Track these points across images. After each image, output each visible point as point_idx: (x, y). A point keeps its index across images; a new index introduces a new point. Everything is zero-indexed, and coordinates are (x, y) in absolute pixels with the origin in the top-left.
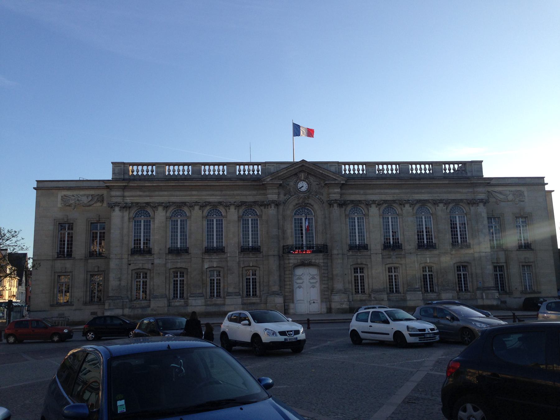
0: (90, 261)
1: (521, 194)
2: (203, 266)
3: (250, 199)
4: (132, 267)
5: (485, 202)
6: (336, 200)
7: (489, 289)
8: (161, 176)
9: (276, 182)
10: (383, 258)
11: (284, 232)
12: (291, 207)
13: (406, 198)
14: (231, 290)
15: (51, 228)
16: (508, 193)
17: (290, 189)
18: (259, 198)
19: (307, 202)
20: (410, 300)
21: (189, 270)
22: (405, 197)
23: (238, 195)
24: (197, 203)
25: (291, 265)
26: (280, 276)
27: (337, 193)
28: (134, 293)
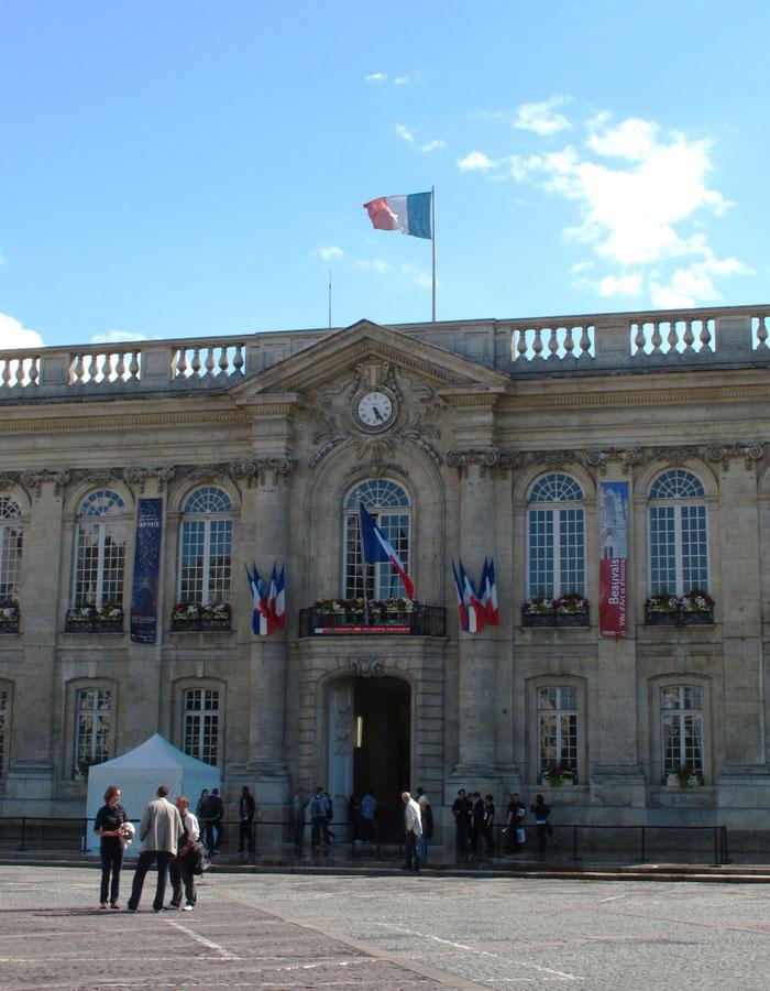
2: (56, 674)
3: (207, 457)
6: (472, 452)
9: (274, 399)
10: (640, 655)
12: (336, 479)
13: (731, 438)
17: (333, 419)
18: (231, 453)
19: (387, 459)
20: (729, 808)
21: (19, 688)
22: (726, 433)
23: (169, 445)
24: (47, 473)
25: (315, 675)
26: (285, 713)
27: (483, 426)
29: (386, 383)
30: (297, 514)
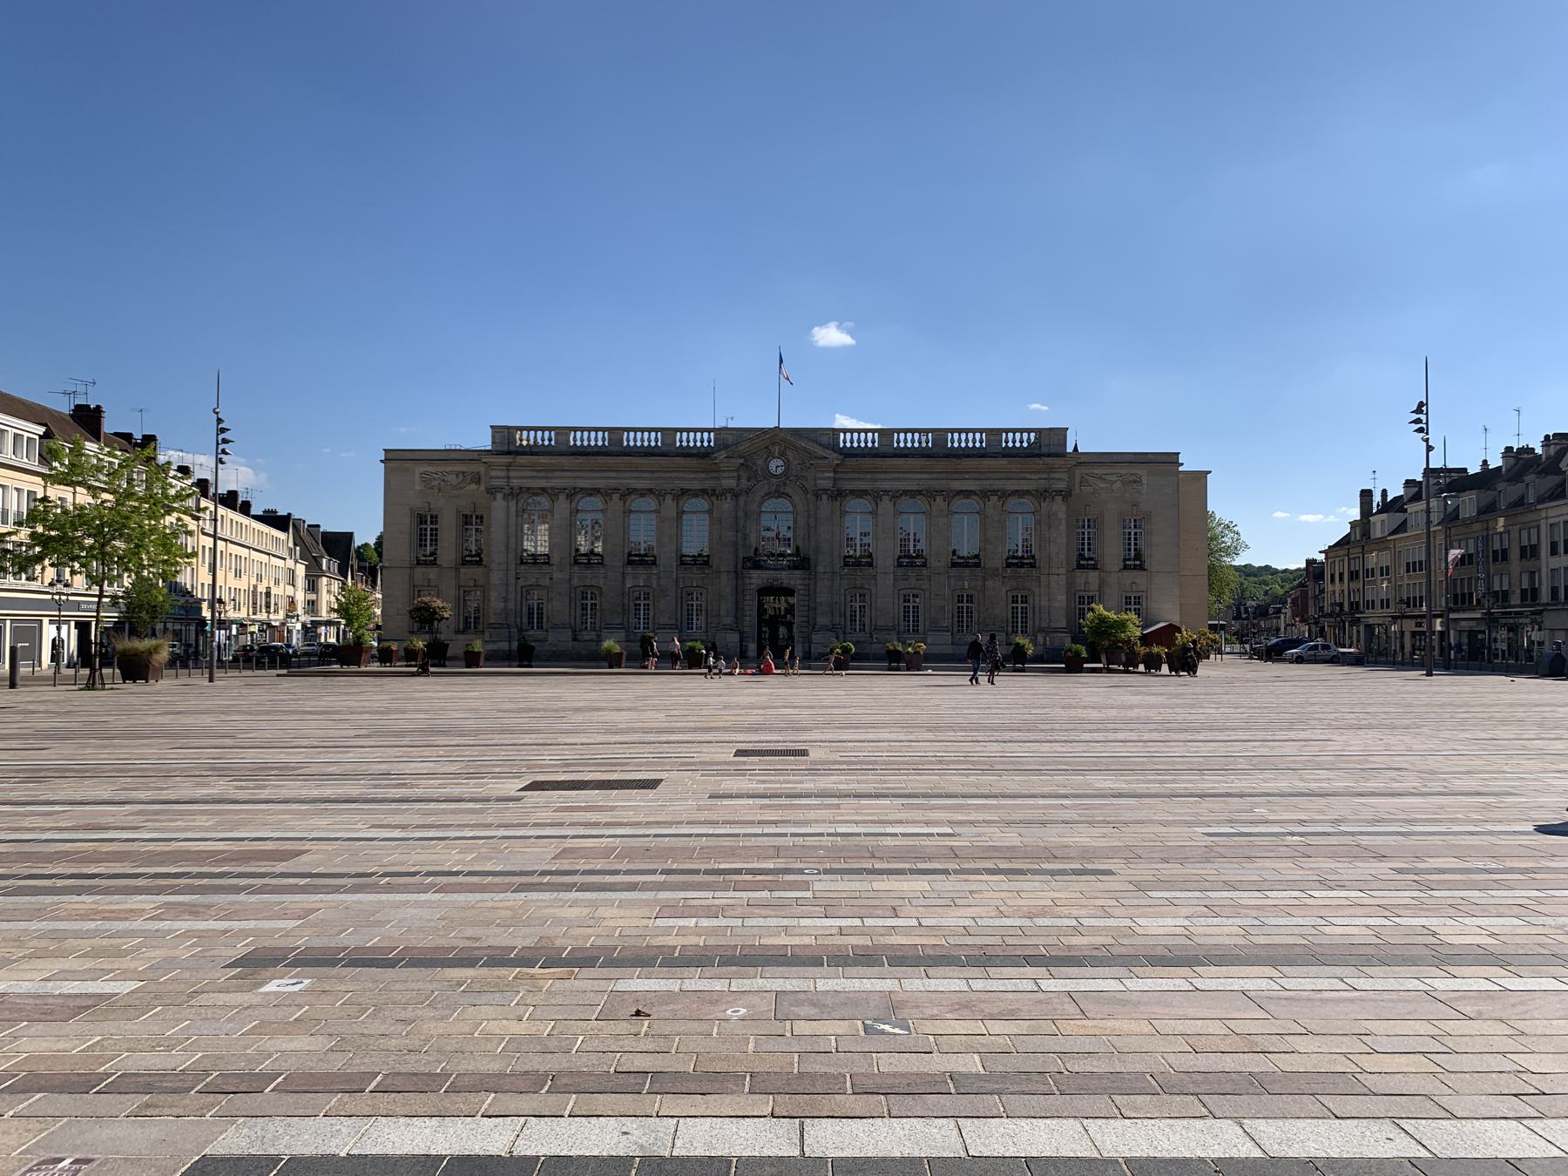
0: (463, 570)
1: (1138, 482)
3: (697, 485)
4: (521, 582)
5: (1066, 495)
7: (1056, 630)
8: (563, 448)
11: (745, 537)
12: (758, 499)
14: (664, 620)
15: (407, 520)
16: (1114, 478)
22: (935, 485)
28: (525, 620)
29: (782, 455)
30: (740, 513)
